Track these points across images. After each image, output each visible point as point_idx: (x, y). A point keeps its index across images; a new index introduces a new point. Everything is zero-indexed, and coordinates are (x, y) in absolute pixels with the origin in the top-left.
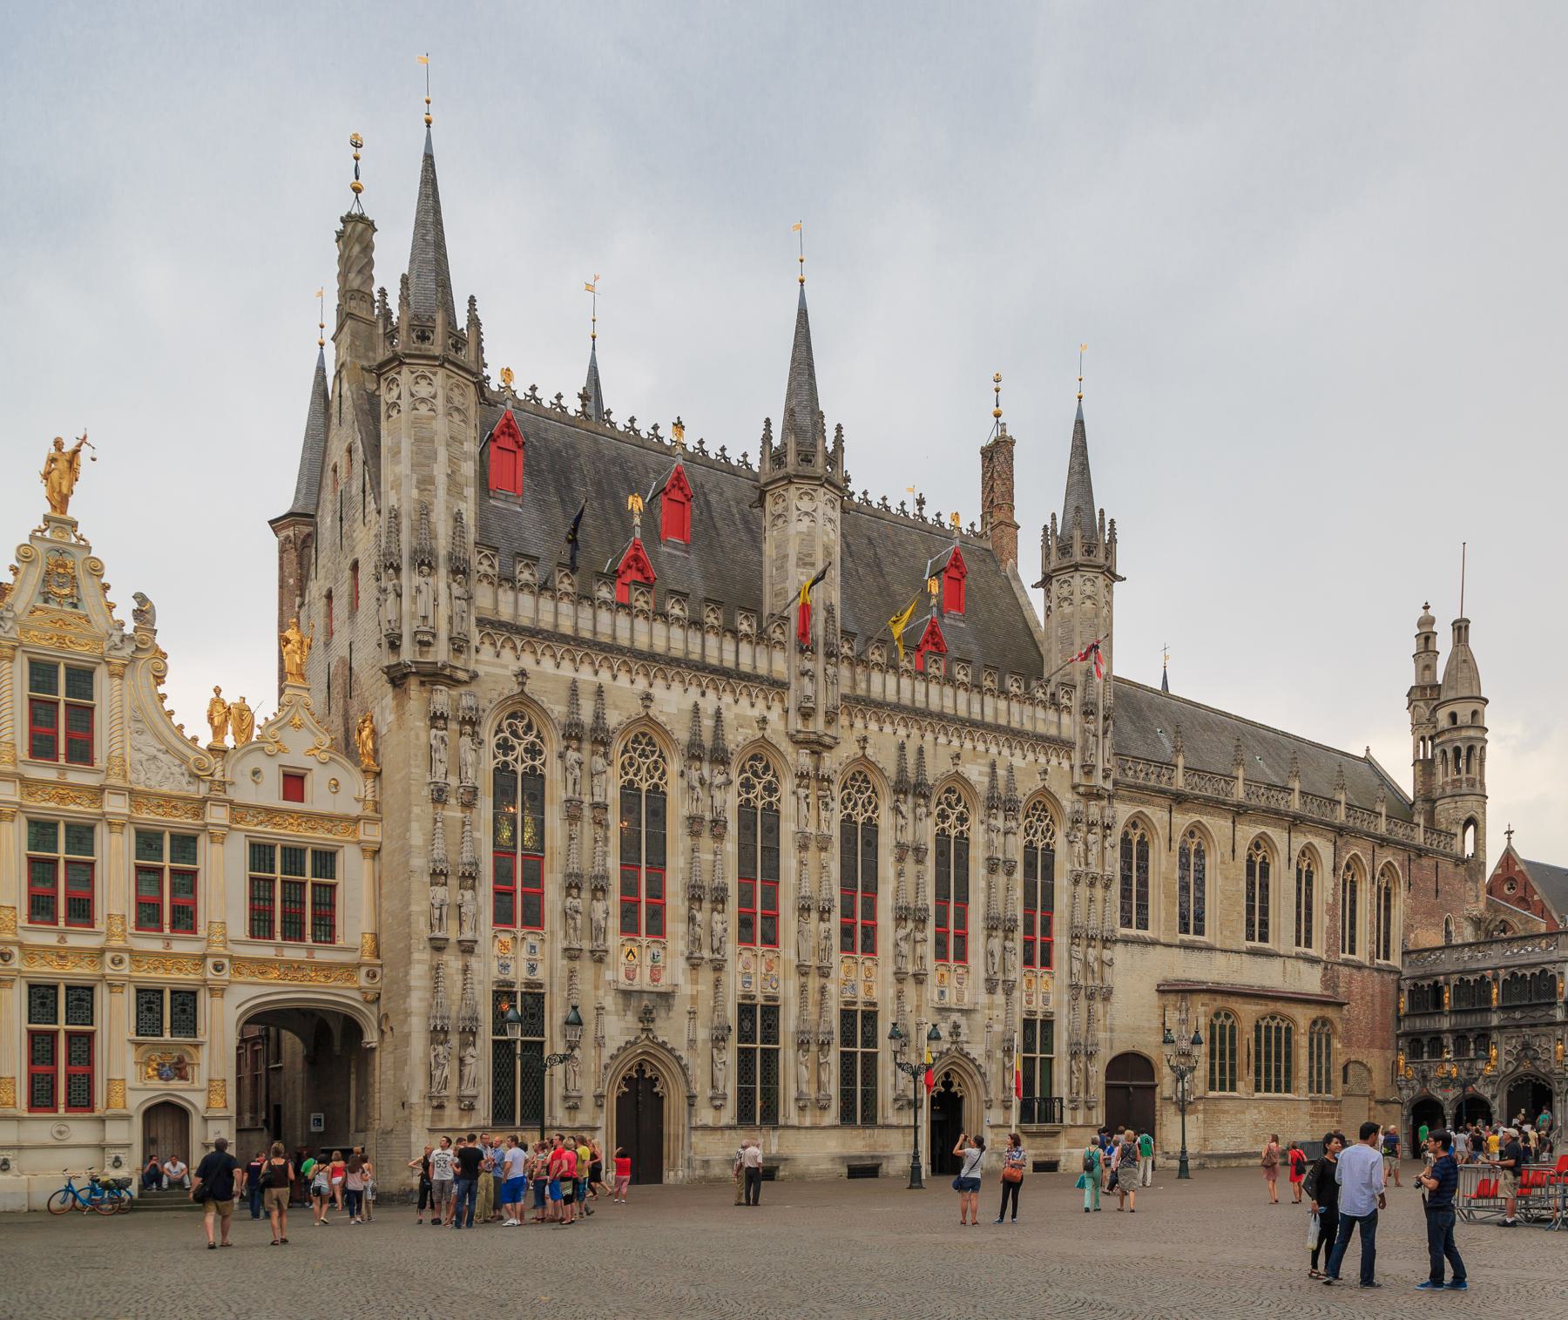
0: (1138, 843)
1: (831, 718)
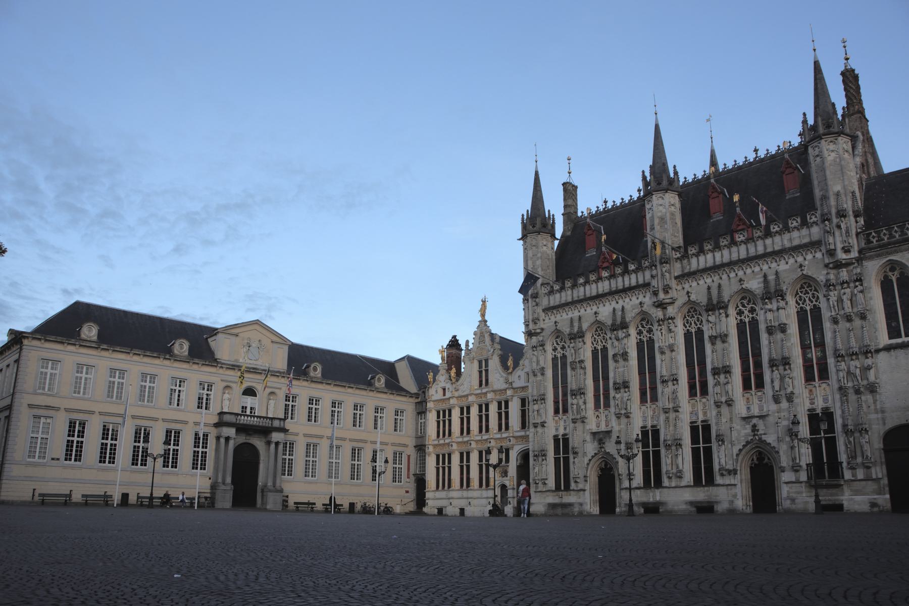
0: (898, 279)
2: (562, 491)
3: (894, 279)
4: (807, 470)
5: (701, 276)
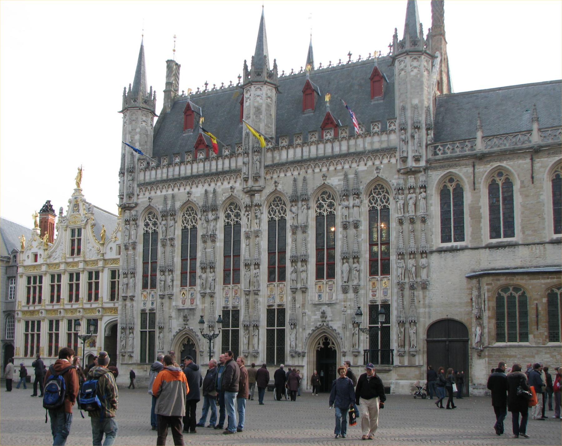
0: (454, 190)
1: (256, 179)
2: (146, 364)
3: (451, 189)
4: (364, 355)
5: (289, 168)
